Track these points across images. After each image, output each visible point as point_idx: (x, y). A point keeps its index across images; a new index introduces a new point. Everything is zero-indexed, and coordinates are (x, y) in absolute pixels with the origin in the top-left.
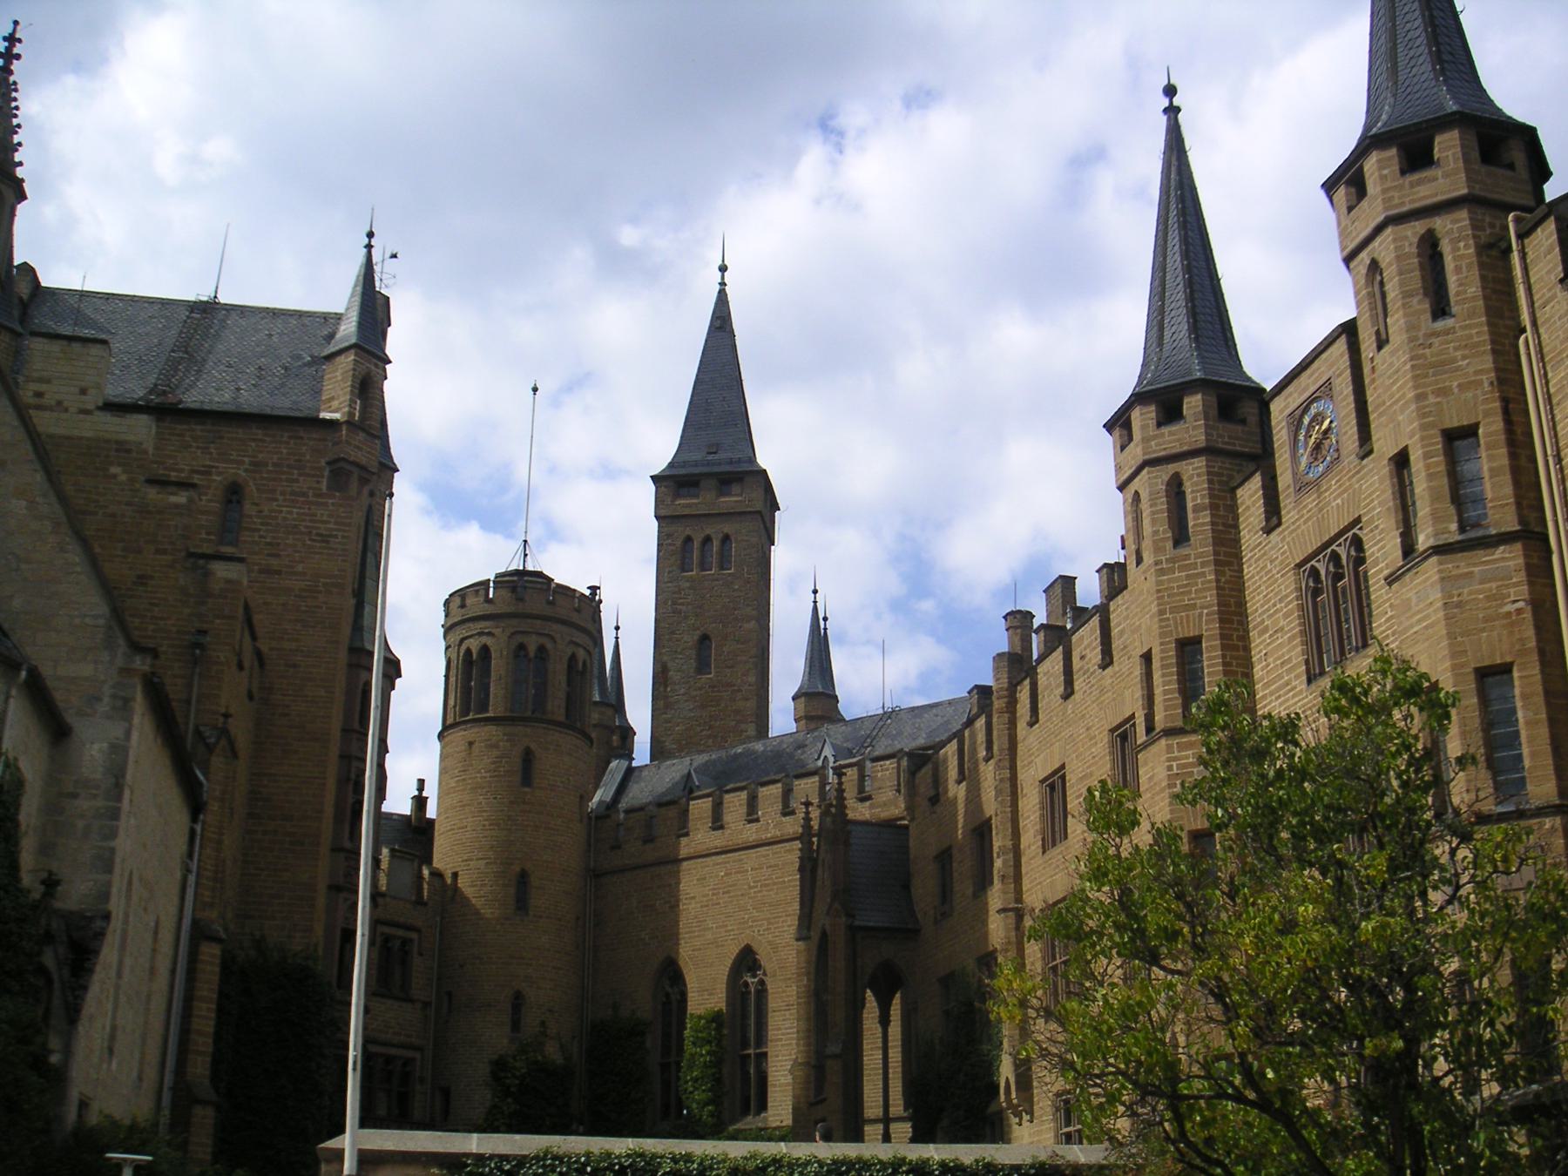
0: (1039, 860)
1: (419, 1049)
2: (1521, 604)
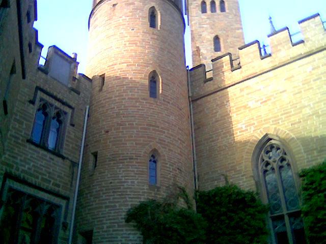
1: (66, 198)
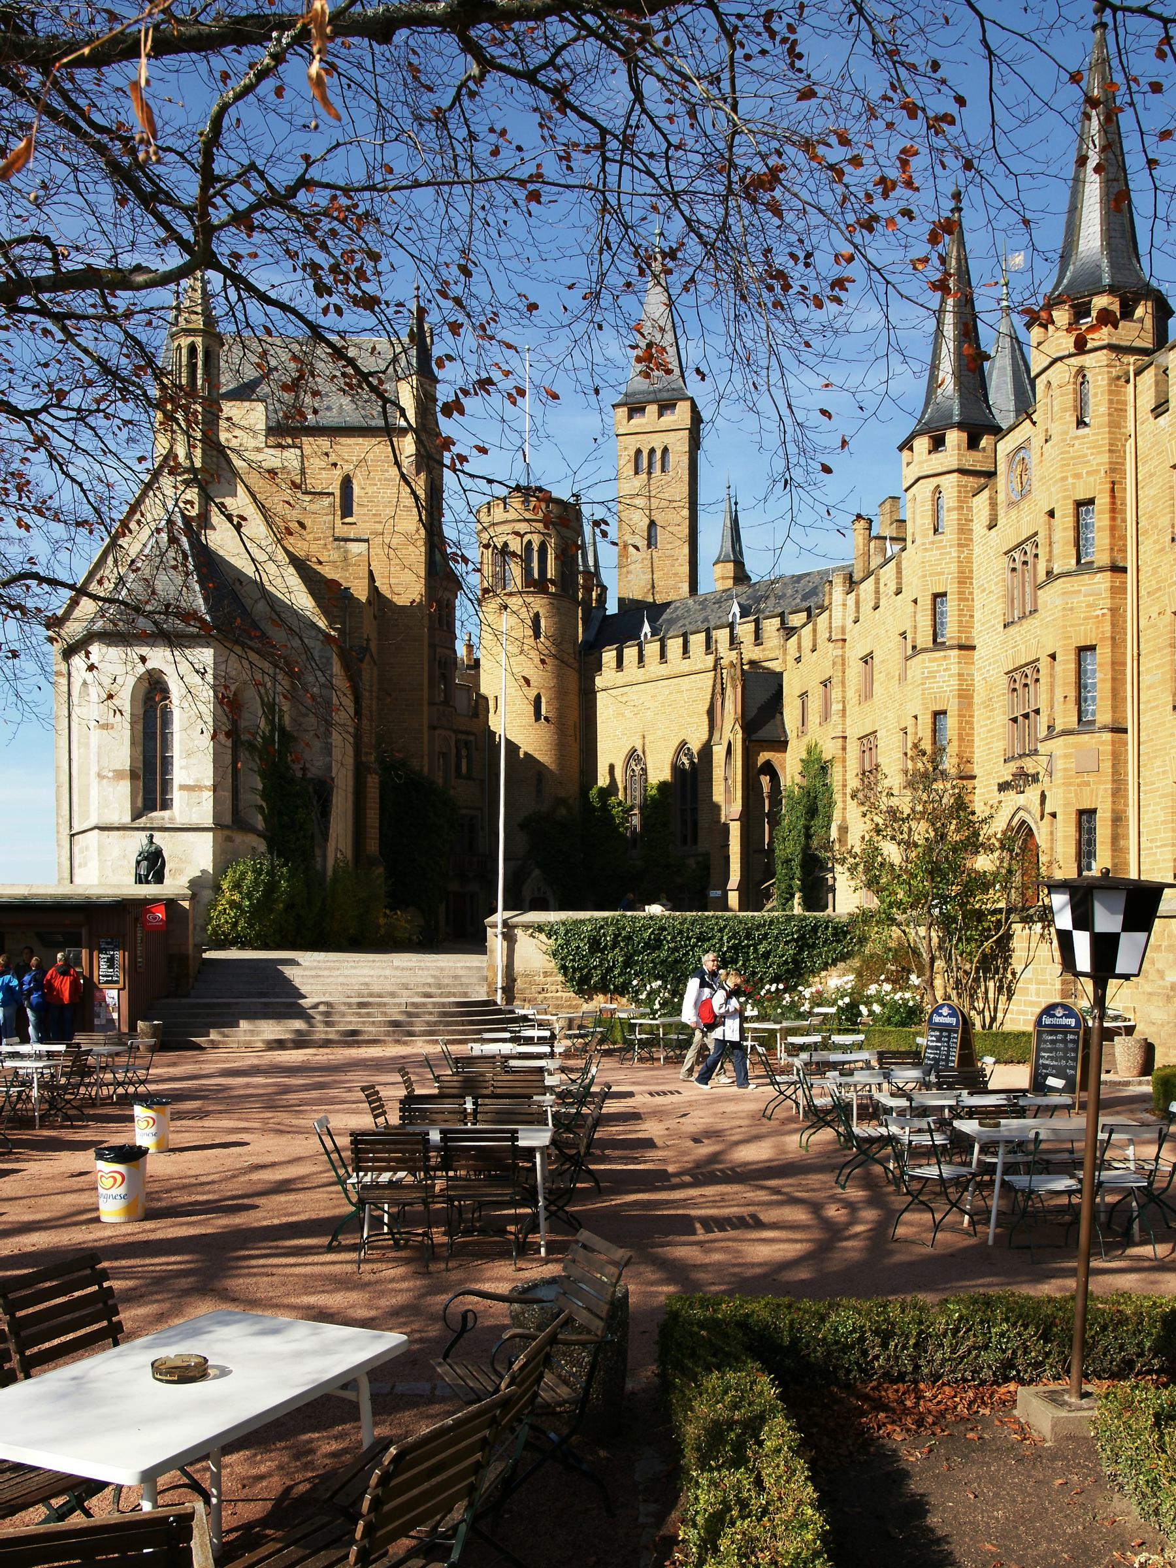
0: (857, 708)
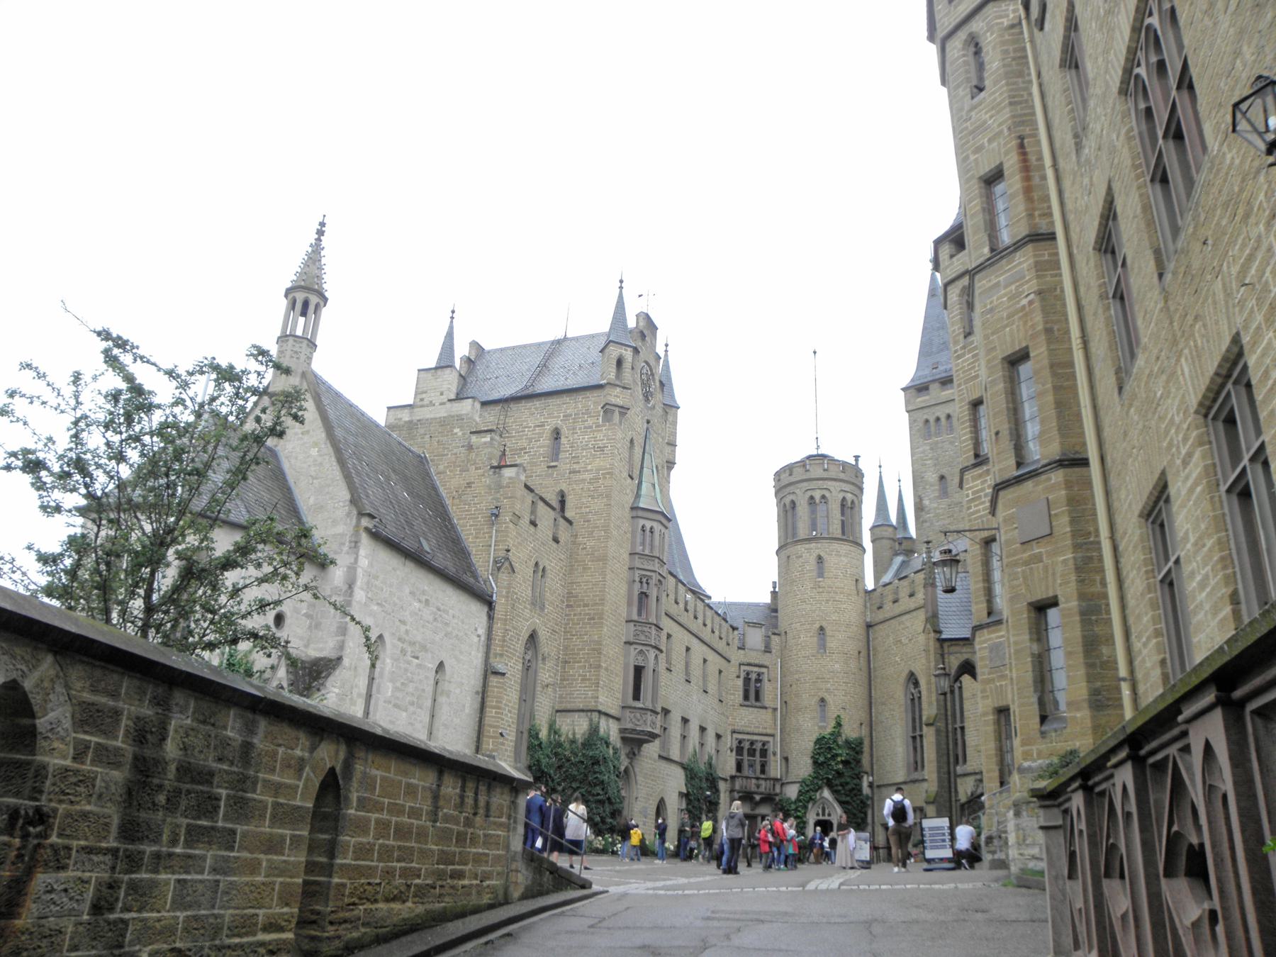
1: (773, 735)
2: (1032, 296)
